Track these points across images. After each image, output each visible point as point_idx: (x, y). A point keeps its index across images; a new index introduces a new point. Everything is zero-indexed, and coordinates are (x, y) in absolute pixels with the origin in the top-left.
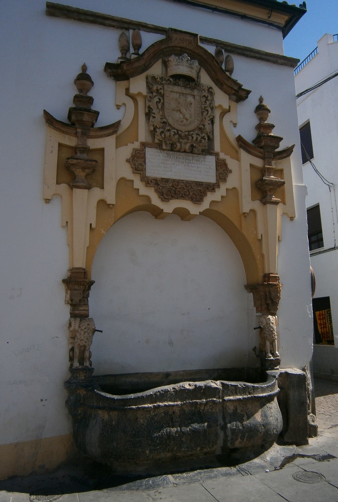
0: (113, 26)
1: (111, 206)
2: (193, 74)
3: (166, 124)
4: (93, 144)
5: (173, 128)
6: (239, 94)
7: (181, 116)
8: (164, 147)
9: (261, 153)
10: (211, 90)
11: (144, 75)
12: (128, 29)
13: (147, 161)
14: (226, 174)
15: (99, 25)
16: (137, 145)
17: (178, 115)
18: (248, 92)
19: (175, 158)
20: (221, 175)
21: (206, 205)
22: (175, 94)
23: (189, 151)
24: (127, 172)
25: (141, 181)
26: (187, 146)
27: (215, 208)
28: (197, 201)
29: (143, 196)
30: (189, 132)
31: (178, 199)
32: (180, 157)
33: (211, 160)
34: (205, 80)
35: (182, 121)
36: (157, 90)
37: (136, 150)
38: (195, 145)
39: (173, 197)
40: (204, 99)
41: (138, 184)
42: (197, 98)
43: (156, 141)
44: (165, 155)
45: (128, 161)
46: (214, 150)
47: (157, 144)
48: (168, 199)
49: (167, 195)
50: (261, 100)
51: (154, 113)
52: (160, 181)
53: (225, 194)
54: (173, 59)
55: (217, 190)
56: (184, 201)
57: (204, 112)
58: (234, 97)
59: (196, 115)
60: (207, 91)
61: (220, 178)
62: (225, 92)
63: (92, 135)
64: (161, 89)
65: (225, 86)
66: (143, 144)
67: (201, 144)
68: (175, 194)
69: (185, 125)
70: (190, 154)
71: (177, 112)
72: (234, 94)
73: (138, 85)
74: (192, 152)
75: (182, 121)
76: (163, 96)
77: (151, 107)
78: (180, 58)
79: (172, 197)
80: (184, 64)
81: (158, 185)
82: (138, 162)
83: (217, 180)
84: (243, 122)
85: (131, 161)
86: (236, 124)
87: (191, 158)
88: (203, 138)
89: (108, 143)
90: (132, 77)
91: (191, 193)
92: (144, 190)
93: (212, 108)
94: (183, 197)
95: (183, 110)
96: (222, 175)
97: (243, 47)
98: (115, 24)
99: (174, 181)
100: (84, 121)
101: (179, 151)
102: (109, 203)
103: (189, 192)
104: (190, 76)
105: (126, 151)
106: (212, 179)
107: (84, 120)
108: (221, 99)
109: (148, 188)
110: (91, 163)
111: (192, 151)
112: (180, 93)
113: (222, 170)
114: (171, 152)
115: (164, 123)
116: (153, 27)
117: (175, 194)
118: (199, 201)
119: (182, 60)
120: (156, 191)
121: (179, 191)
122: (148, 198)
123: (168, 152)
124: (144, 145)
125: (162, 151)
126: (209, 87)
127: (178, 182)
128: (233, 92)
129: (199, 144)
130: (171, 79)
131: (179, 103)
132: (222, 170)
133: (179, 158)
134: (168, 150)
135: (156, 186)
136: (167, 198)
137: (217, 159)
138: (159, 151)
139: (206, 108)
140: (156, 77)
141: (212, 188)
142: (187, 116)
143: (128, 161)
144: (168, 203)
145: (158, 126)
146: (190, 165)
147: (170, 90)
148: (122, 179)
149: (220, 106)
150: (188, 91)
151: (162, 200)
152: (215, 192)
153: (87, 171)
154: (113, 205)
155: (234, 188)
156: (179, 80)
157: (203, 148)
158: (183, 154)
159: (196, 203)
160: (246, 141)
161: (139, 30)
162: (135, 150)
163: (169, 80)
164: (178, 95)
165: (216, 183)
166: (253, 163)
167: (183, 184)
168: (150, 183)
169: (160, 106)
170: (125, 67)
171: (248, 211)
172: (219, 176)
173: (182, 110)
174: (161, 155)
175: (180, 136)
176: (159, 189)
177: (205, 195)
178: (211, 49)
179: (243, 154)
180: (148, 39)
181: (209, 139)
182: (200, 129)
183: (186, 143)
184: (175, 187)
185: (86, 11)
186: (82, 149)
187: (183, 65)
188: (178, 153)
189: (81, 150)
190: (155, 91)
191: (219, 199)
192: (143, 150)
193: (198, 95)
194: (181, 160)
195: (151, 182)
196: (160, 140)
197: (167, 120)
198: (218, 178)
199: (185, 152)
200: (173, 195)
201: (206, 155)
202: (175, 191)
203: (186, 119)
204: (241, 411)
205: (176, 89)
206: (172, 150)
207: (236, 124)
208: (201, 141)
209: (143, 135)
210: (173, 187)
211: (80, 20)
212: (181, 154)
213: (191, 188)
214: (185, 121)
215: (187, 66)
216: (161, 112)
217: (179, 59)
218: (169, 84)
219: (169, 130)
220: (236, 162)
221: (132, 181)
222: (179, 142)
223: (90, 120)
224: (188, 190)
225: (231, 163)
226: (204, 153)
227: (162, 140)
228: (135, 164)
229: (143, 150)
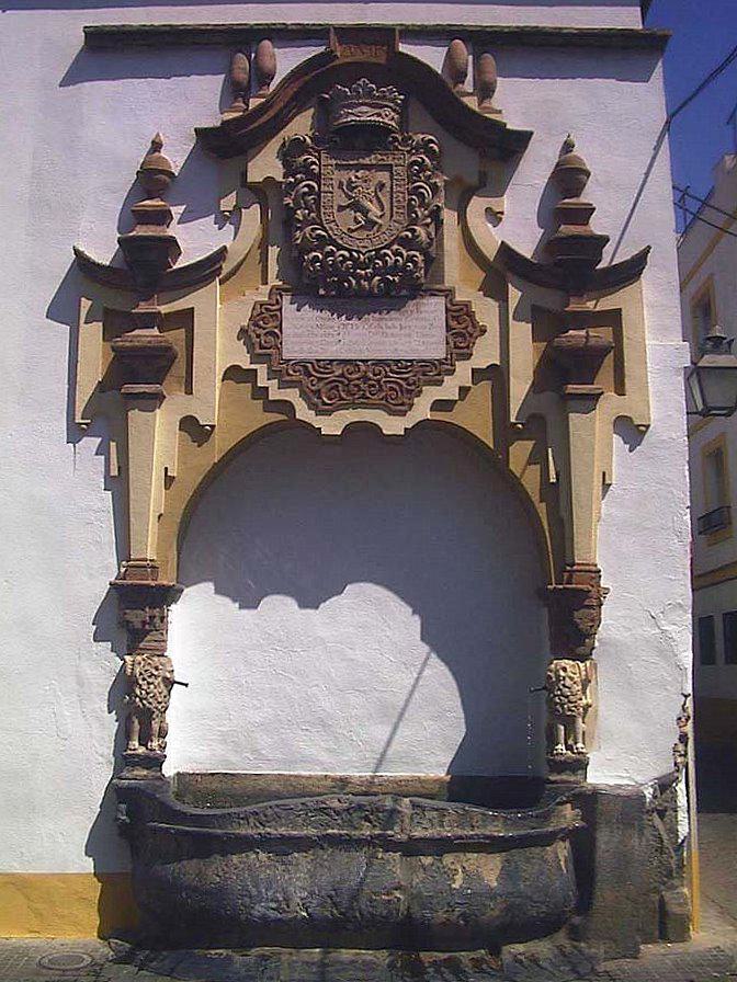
5: (340, 248)
6: (502, 148)
18: (523, 139)
21: (422, 410)
33: (434, 308)
50: (568, 147)
59: (395, 209)
73: (265, 166)
103: (381, 386)
106: (439, 353)
121: (356, 386)
141: (434, 371)
146: (383, 324)
165: (446, 359)
173: (360, 207)
178: (433, 57)
180: (286, 61)
181: (429, 260)
219: (332, 253)
225: (486, 312)
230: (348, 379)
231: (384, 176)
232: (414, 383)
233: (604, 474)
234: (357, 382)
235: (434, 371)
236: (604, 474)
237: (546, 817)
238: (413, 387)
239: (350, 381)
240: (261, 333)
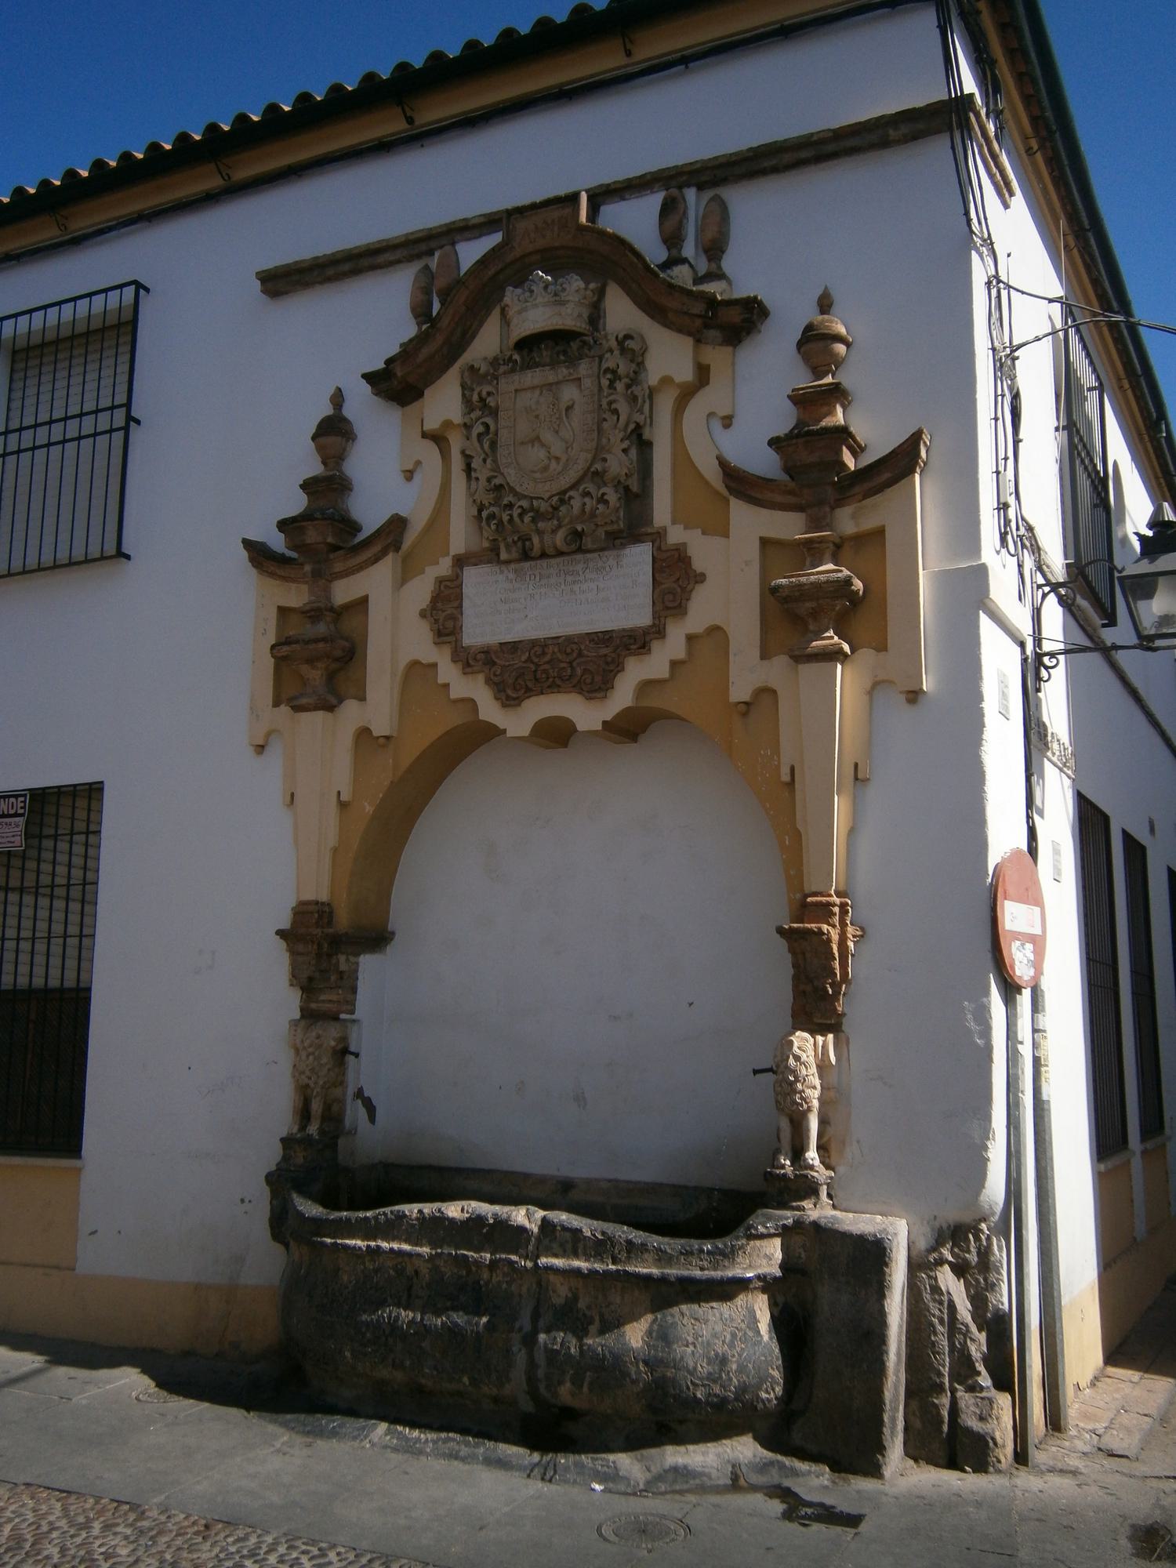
0: (399, 262)
1: (382, 741)
2: (569, 317)
4: (343, 592)
5: (520, 496)
7: (542, 454)
8: (504, 556)
10: (629, 344)
12: (430, 253)
13: (466, 603)
14: (683, 589)
17: (537, 454)
21: (622, 696)
23: (573, 547)
24: (419, 644)
27: (648, 703)
28: (596, 691)
29: (463, 700)
33: (639, 557)
34: (621, 313)
35: (546, 468)
36: (482, 400)
38: (579, 529)
39: (529, 692)
40: (605, 382)
41: (448, 672)
42: (587, 383)
43: (486, 544)
44: (511, 576)
49: (515, 689)
53: (681, 654)
55: (655, 645)
58: (713, 333)
60: (617, 352)
61: (668, 608)
62: (680, 331)
64: (489, 394)
70: (579, 557)
72: (706, 326)
73: (444, 402)
74: (579, 550)
75: (546, 468)
76: (494, 412)
79: (528, 690)
80: (540, 300)
83: (656, 615)
84: (751, 404)
87: (580, 567)
88: (602, 500)
91: (579, 671)
95: (547, 436)
96: (671, 597)
97: (750, 149)
98: (398, 254)
99: (534, 643)
101: (544, 555)
102: (375, 733)
105: (421, 591)
106: (642, 618)
107: (308, 541)
108: (669, 356)
111: (577, 545)
112: (541, 387)
113: (675, 579)
114: (527, 564)
115: (499, 488)
116: (482, 220)
118: (599, 689)
119: (532, 291)
121: (545, 671)
122: (471, 704)
124: (460, 562)
125: (504, 568)
126: (621, 336)
129: (611, 514)
132: (675, 579)
134: (519, 560)
137: (659, 548)
138: (497, 568)
139: (614, 406)
140: (476, 366)
141: (637, 642)
142: (557, 449)
146: (576, 588)
147: (512, 388)
148: (415, 664)
149: (666, 381)
150: (563, 372)
151: (504, 706)
154: (387, 738)
157: (609, 528)
158: (559, 560)
162: (440, 581)
166: (772, 534)
171: (746, 698)
174: (501, 577)
175: (538, 516)
179: (741, 514)
182: (596, 473)
183: (554, 532)
187: (536, 306)
188: (544, 562)
192: (457, 576)
199: (561, 554)
200: (530, 685)
201: (623, 546)
203: (557, 459)
204: (589, 1307)
205: (532, 377)
206: (526, 556)
209: (460, 535)
212: (553, 561)
213: (580, 655)
216: (489, 461)
218: (513, 371)
219: (510, 506)
221: (435, 665)
224: (570, 663)
225: (703, 551)
226: (618, 542)
228: (436, 621)
231: (569, 393)
232: (613, 661)
233: (856, 765)
234: (546, 667)
235: (637, 642)
236: (856, 765)
237: (729, 1255)
239: (537, 665)
240: (444, 612)
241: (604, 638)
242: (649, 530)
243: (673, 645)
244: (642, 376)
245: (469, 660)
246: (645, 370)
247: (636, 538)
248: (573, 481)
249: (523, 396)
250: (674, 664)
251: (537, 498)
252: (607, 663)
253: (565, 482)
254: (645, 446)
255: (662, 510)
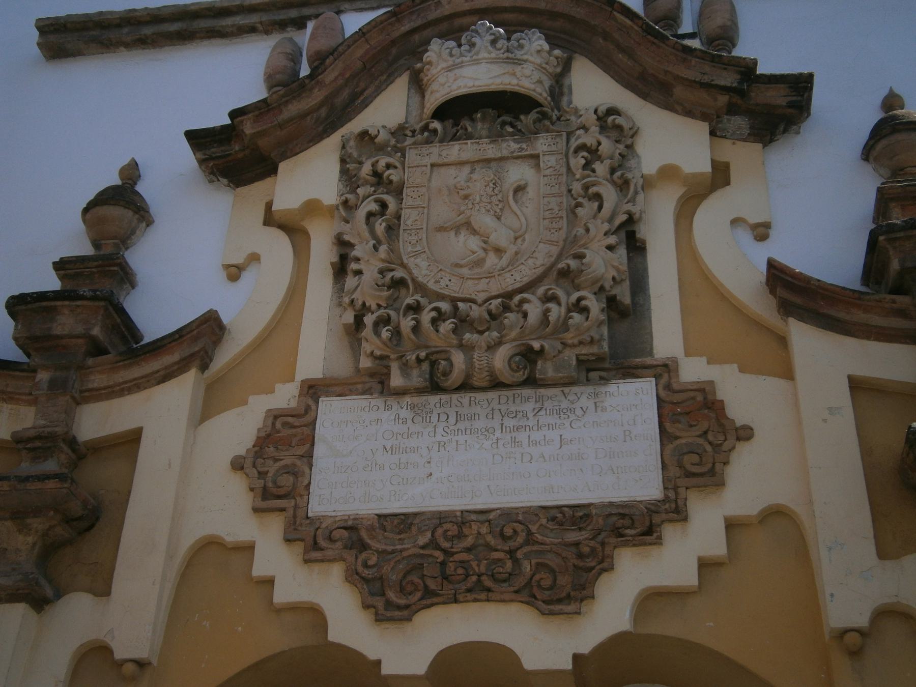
0: (252, 30)
1: (130, 668)
3: (408, 288)
4: (95, 422)
7: (474, 243)
8: (396, 380)
9: (901, 313)
11: (333, 141)
12: (300, 24)
13: (319, 450)
14: (716, 447)
15: (206, 42)
16: (285, 396)
17: (464, 245)
19: (452, 420)
20: (689, 460)
21: (611, 610)
22: (452, 171)
23: (520, 376)
24: (226, 508)
25: (288, 540)
26: (500, 359)
27: (658, 627)
28: (559, 601)
29: (293, 608)
30: (509, 295)
31: (456, 601)
32: (478, 409)
33: (633, 402)
35: (479, 263)
36: (376, 174)
37: (276, 417)
38: (536, 345)
39: (431, 597)
40: (578, 162)
41: (274, 557)
42: (550, 161)
43: (366, 363)
44: (405, 413)
45: (237, 465)
46: (651, 353)
47: (372, 374)
48: (407, 607)
49: (402, 590)
51: (357, 260)
52: (371, 529)
53: (717, 547)
54: (437, 52)
55: (669, 532)
56: (491, 609)
57: (579, 205)
58: (740, 123)
60: (595, 129)
61: (690, 475)
62: (689, 113)
63: (95, 385)
64: (388, 166)
65: (679, 91)
66: (310, 387)
67: (569, 337)
68: (445, 577)
69: (490, 276)
70: (527, 392)
71: (457, 233)
72: (732, 110)
73: (311, 178)
74: (531, 382)
75: (479, 263)
76: (398, 191)
77: (346, 238)
78: (463, 41)
79: (428, 593)
80: (483, 55)
81: (363, 547)
82: (278, 464)
83: (668, 483)
85: (248, 463)
86: (767, 226)
87: (529, 407)
88: (579, 307)
89: (161, 411)
90: (285, 157)
91: (527, 567)
92: (294, 579)
93: (623, 186)
94: (479, 588)
95: (483, 220)
96: (695, 458)
98: (253, 19)
99: (441, 518)
100: (58, 337)
101: (465, 386)
102: (119, 655)
103: (516, 562)
104: (509, 88)
105: (238, 428)
106: (642, 483)
107: (58, 330)
108: (671, 142)
109: (317, 567)
110: (38, 485)
111: (529, 372)
112: (472, 163)
113: (698, 436)
114: (434, 399)
115: (398, 284)
117: (445, 577)
118: (568, 598)
119: (473, 45)
120: (353, 577)
122: (314, 616)
123: (417, 400)
124: (314, 390)
125: (391, 401)
126: (602, 109)
127: (460, 521)
128: (723, 99)
130: (436, 125)
131: (466, 197)
133: (472, 418)
134: (420, 391)
135: (350, 556)
136: (402, 602)
137: (668, 387)
138: (379, 402)
139: (593, 190)
140: (373, 132)
141: (638, 526)
142: (500, 236)
143: (237, 465)
144: (408, 626)
145: (372, 303)
146: (522, 436)
147: (427, 161)
148: (210, 545)
149: (668, 173)
150: (510, 146)
151: (379, 619)
152: (659, 541)
153: (38, 524)
154: (141, 664)
155: (775, 514)
156: (473, 120)
157: (584, 350)
158: (492, 395)
159: (552, 613)
160: (808, 280)
161: (339, 12)
162: (275, 416)
163: (426, 128)
164: (467, 169)
165: (666, 500)
166: (863, 371)
167: (484, 530)
168: (322, 543)
169: (380, 227)
170: (249, 128)
171: (862, 621)
172: (681, 466)
174: (386, 415)
175: (463, 323)
176: (366, 565)
177: (606, 565)
179: (807, 341)
182: (565, 273)
183: (491, 348)
184: (446, 545)
185: (158, 9)
186: (38, 444)
187: (477, 62)
188: (465, 398)
189: (34, 449)
190: (366, 182)
191: (688, 577)
192: (308, 409)
193: (551, 153)
194: (480, 424)
195: (331, 539)
196: (378, 353)
197: (410, 273)
198: (674, 471)
199: (496, 384)
200: (432, 585)
201: (605, 380)
202: (443, 564)
203: (499, 251)
205: (455, 151)
206: (435, 387)
207: (767, 226)
208: (564, 326)
209: (317, 348)
210: (438, 547)
211: (143, 43)
212: (480, 396)
213: (530, 539)
214: (492, 260)
215: (493, 61)
216: (383, 248)
217: (460, 46)
218: (428, 142)
219: (416, 308)
220: (771, 385)
221: (248, 549)
222: (461, 346)
223: (80, 329)
224: (511, 553)
225: (744, 395)
226: (594, 375)
227: (387, 352)
228: (262, 475)
229: (308, 409)
230: (445, 551)
231: (518, 173)
234: (464, 556)
235: (638, 526)
238: (590, 563)
240: (278, 466)
241: (574, 516)
242: (648, 361)
243: (701, 533)
244: (632, 163)
245: (315, 541)
246: (636, 155)
247: (629, 372)
248: (526, 280)
249: (441, 177)
250: (705, 565)
251: (464, 300)
252: (581, 556)
253: (512, 280)
254: (635, 247)
255: (666, 334)
